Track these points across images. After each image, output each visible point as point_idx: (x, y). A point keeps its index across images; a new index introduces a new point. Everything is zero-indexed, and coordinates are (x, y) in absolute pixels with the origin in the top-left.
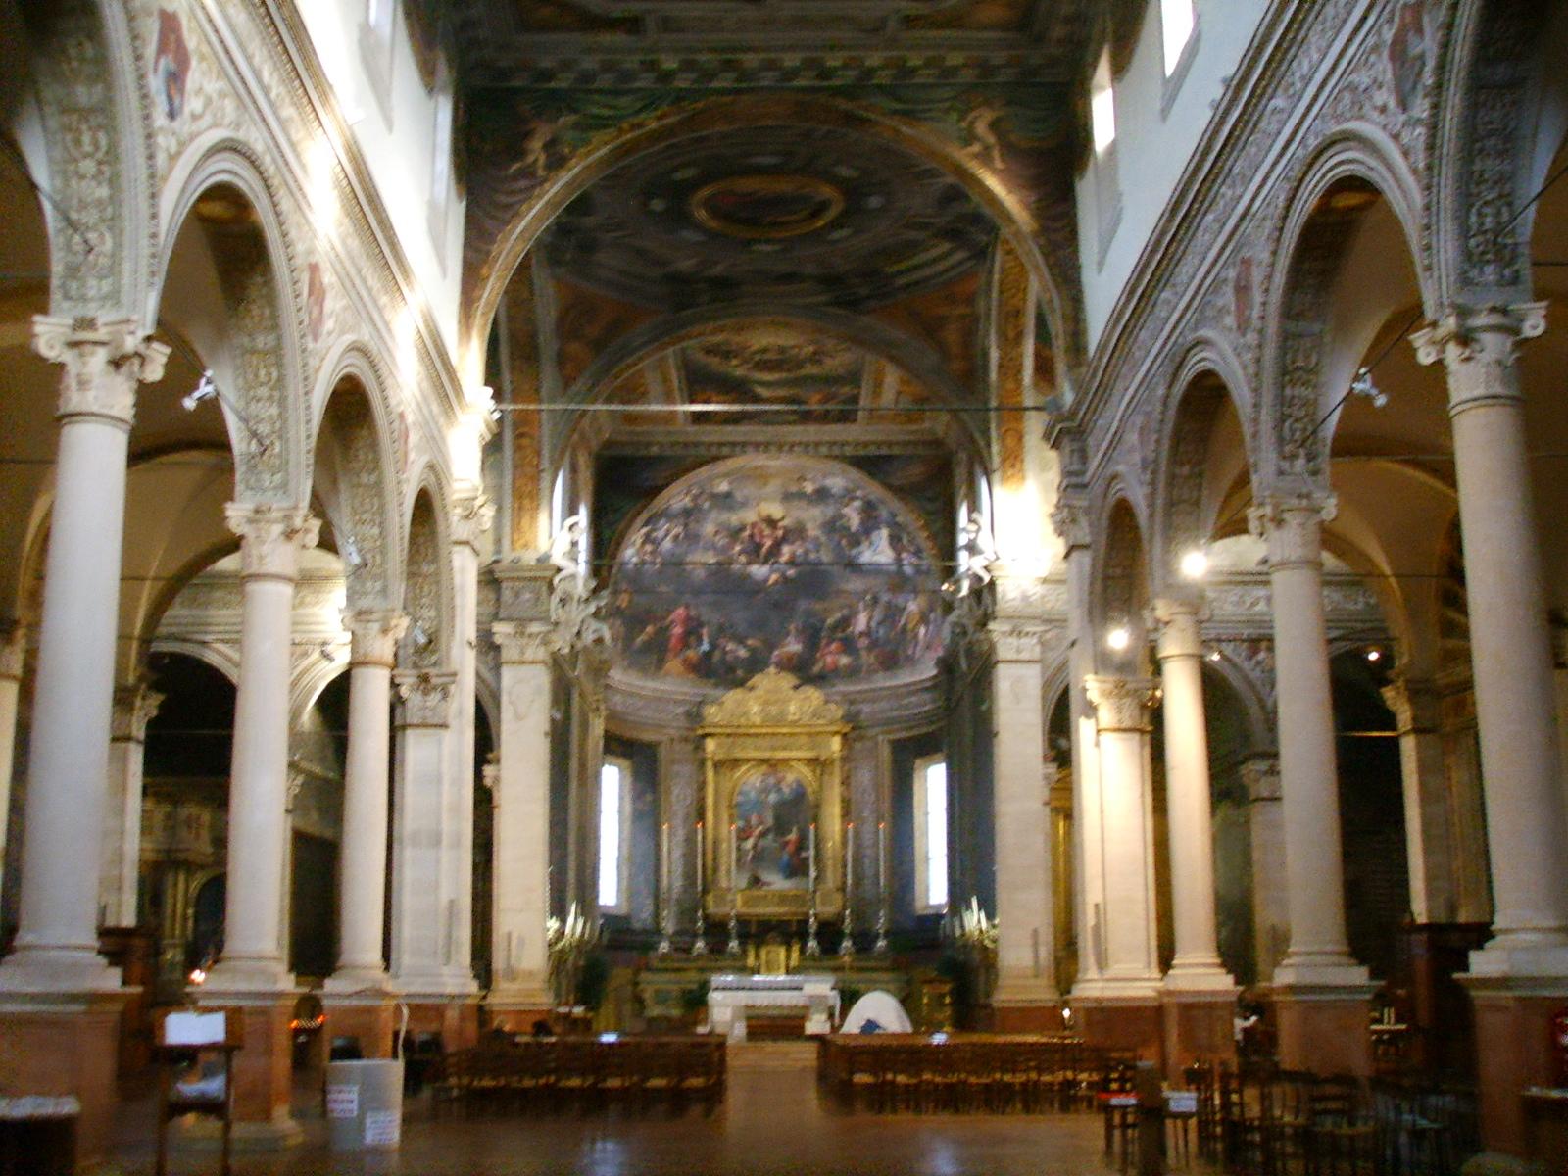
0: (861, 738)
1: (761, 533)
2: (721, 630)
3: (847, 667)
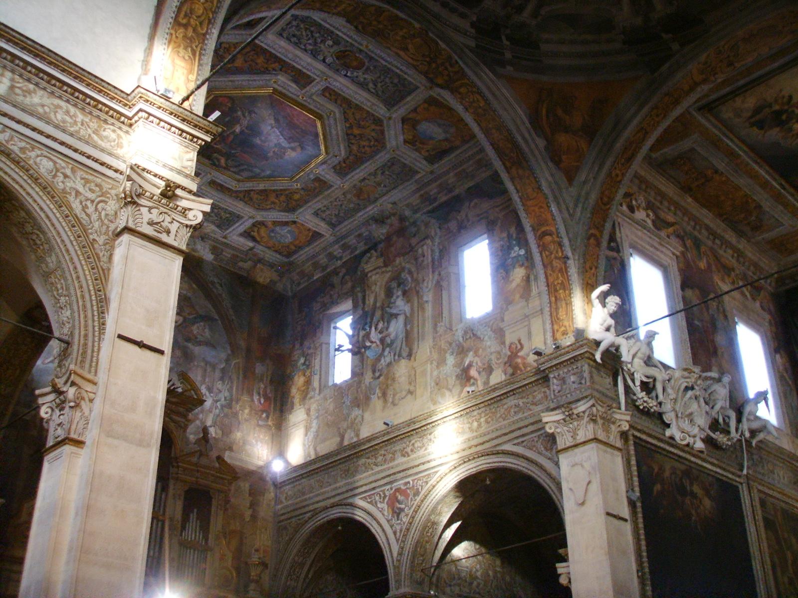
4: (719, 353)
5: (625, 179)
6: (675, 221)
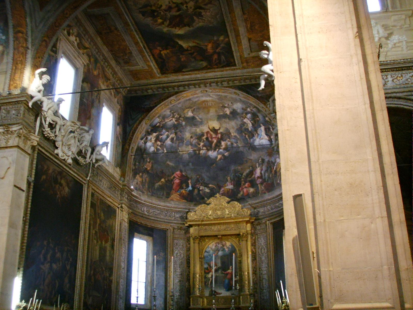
0: (259, 224)
1: (211, 135)
2: (197, 180)
3: (253, 193)
4: (92, 119)
5: (71, 17)
6: (88, 47)
